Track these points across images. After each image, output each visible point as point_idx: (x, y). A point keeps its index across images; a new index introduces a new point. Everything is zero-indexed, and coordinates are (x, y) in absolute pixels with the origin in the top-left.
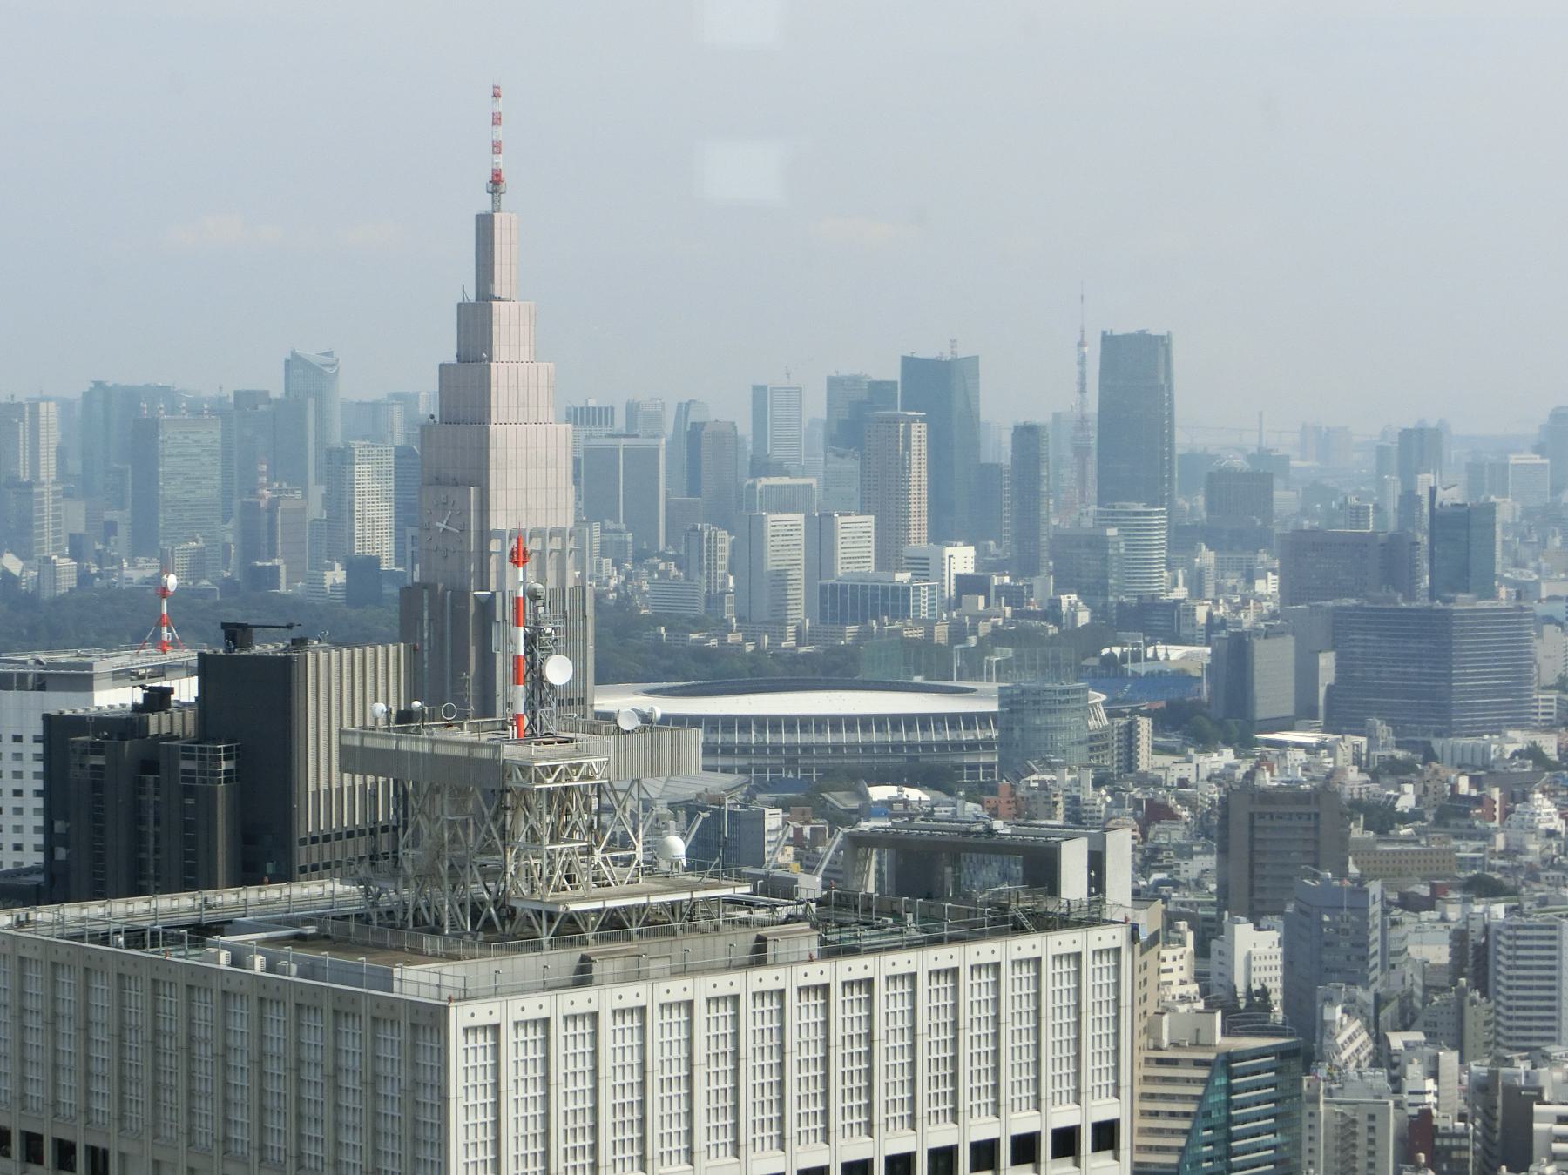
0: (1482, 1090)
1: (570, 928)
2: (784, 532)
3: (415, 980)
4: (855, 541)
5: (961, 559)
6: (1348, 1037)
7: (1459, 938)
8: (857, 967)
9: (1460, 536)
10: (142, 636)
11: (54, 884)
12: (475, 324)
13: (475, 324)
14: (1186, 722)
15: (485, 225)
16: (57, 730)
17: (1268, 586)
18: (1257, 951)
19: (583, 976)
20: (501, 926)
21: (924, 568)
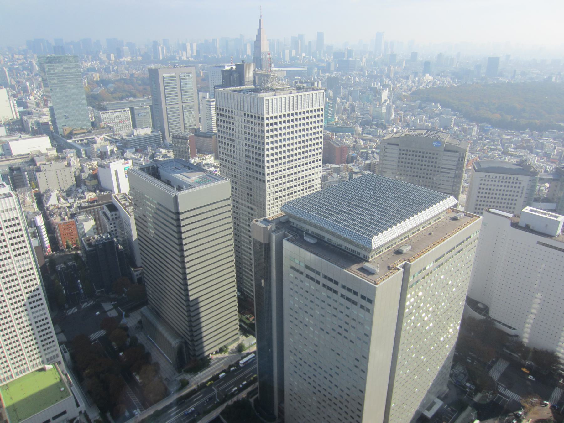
0: (350, 105)
1: (274, 90)
2: (287, 52)
3: (261, 95)
4: (294, 53)
5: (303, 55)
6: (339, 100)
7: (349, 91)
8: (300, 94)
9: (350, 52)
10: (229, 62)
11: (222, 86)
12: (259, 30)
13: (259, 30)
14: (324, 70)
15: (260, 21)
16: (223, 71)
17: (332, 57)
18: (331, 92)
19: (275, 95)
20: (268, 90)
21: (300, 55)
